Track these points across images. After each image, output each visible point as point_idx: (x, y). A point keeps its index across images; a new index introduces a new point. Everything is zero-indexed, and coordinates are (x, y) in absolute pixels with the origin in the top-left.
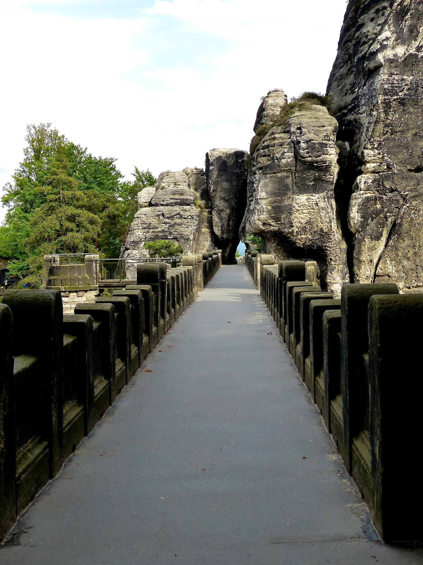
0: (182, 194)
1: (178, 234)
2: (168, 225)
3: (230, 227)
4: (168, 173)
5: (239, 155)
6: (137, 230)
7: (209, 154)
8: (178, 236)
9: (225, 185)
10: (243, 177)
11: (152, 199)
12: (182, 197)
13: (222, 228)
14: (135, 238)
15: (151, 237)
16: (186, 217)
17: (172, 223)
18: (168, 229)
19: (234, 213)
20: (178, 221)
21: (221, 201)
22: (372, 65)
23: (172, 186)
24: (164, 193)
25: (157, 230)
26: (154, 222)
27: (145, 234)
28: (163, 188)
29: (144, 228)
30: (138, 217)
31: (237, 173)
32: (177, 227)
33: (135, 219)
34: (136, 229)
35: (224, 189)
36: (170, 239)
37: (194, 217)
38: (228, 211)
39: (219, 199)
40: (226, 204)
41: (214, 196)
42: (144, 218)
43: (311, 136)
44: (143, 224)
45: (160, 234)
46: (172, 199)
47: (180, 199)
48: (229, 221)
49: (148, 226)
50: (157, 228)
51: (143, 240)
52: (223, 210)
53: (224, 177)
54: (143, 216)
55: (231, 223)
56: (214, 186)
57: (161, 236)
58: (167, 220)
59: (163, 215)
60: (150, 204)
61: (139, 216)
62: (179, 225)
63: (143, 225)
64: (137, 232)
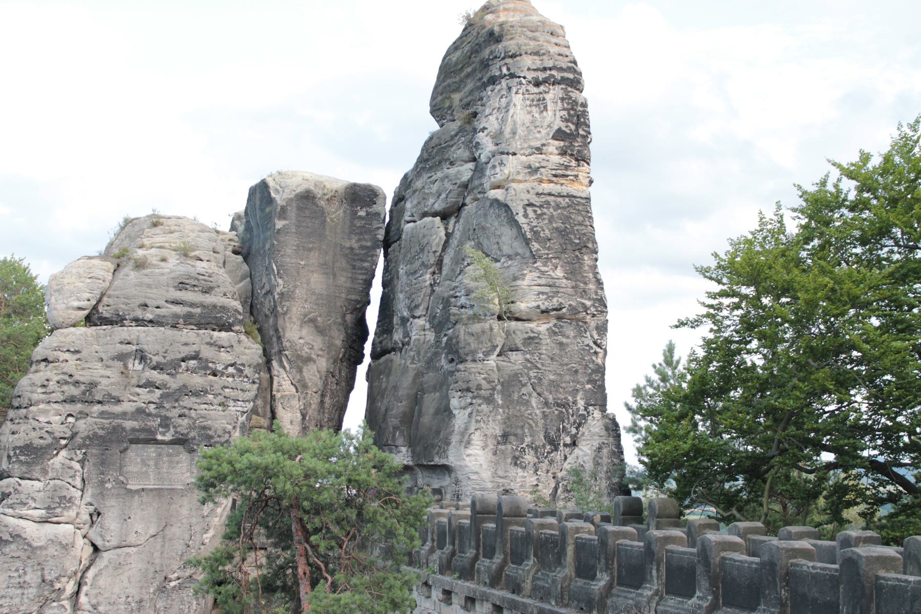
0: (207, 291)
1: (191, 428)
2: (158, 393)
3: (324, 413)
4: (156, 222)
5: (361, 196)
6: (42, 406)
7: (271, 183)
8: (192, 434)
9: (317, 281)
10: (366, 264)
11: (99, 301)
12: (209, 299)
13: (304, 416)
14: (33, 434)
15: (95, 434)
16: (220, 367)
17: (174, 384)
18: (160, 406)
19: (337, 372)
20: (197, 380)
21: (304, 332)
23: (173, 260)
24: (146, 280)
25: (117, 409)
26: (107, 378)
27: (70, 419)
28: (140, 265)
29: (72, 400)
30: (45, 360)
31: (352, 249)
32: (188, 401)
33: (34, 367)
34: (37, 403)
35: (313, 293)
36: (163, 443)
37: (247, 371)
38: (323, 364)
39: (298, 323)
40: (318, 342)
41: (285, 314)
42: (72, 364)
44: (67, 383)
45: (129, 424)
46: (175, 302)
47: (202, 306)
48: (323, 396)
49: (84, 393)
50: (118, 401)
51: (63, 442)
52: (309, 360)
53: (314, 258)
54: (67, 356)
55: (327, 400)
56: (285, 281)
57: (134, 430)
58: (155, 375)
59: (142, 356)
61: (51, 355)
62: (196, 394)
63: (65, 388)
64: (45, 412)
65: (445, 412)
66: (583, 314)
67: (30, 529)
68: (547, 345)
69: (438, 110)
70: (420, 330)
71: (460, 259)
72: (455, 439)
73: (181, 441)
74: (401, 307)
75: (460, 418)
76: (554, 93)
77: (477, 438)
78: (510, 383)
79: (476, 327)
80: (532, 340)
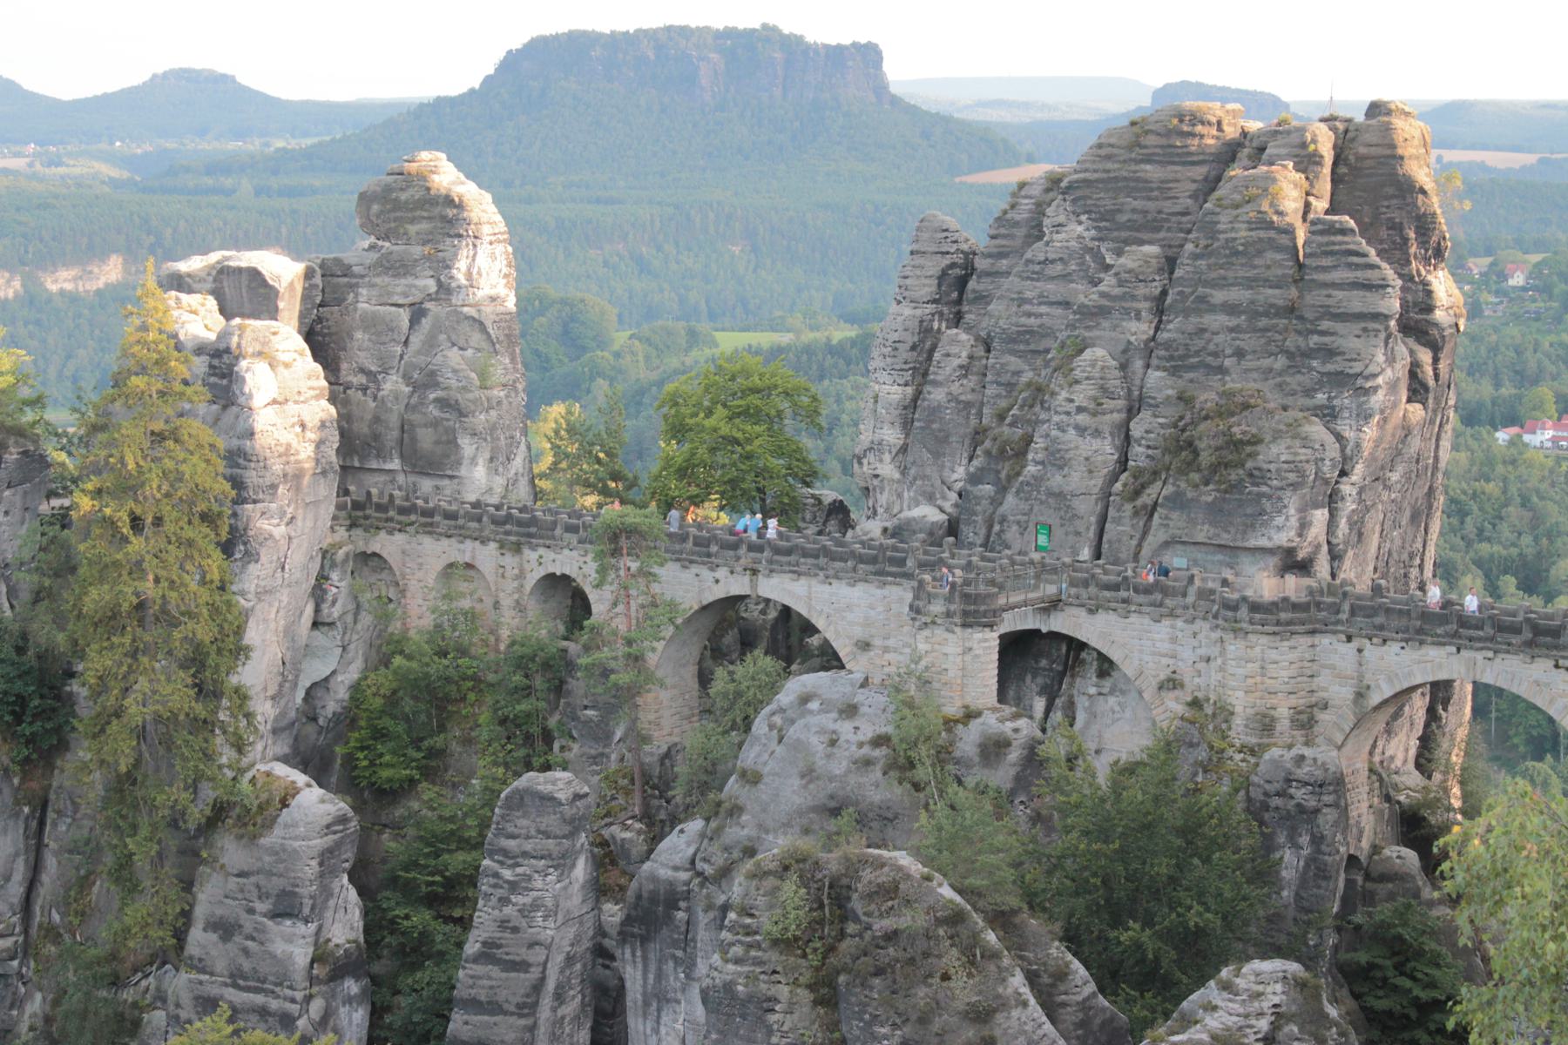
72: (466, 462)
77: (481, 461)
78: (493, 428)
79: (470, 396)
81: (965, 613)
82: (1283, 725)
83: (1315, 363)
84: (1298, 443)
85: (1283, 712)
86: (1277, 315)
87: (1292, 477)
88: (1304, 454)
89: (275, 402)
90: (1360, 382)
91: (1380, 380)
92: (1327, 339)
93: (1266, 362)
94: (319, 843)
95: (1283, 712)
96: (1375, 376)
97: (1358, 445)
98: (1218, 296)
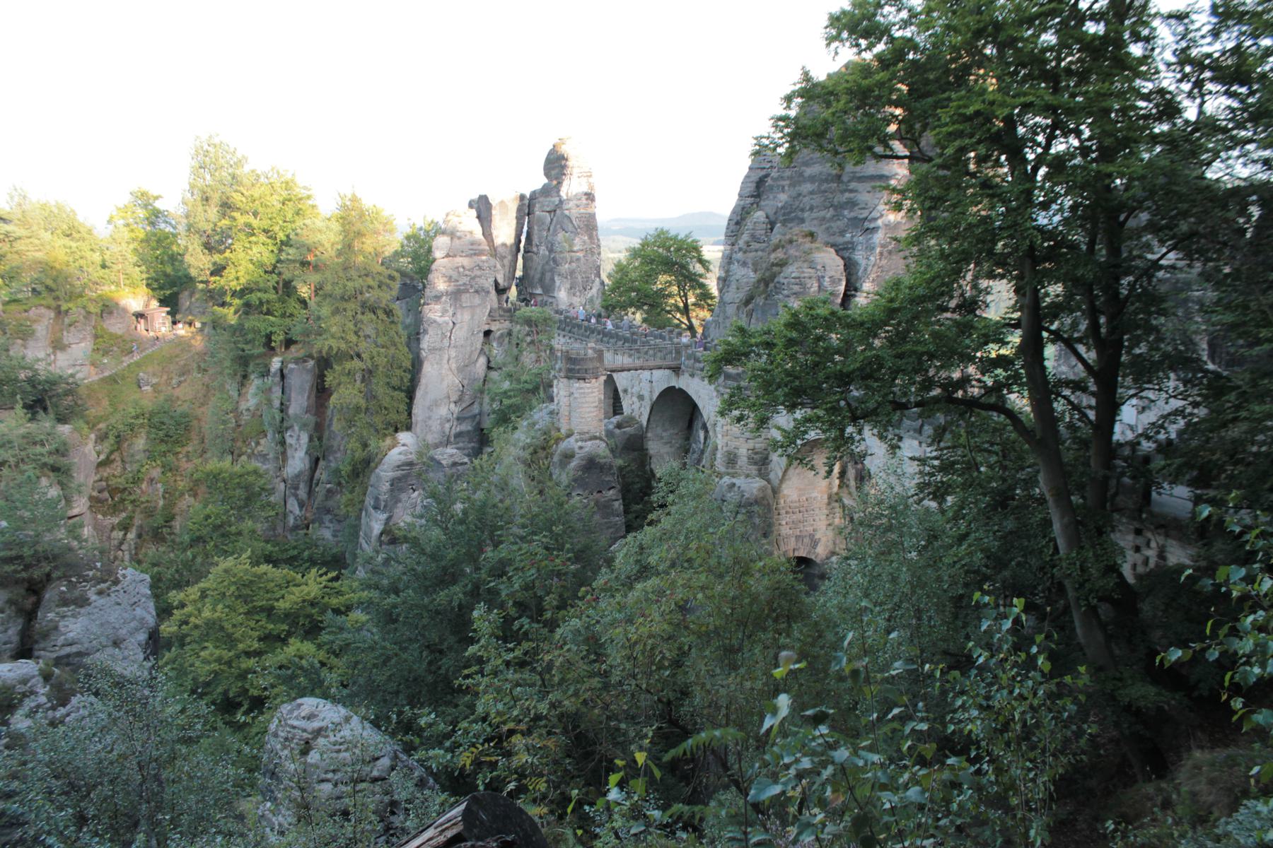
20: (479, 273)
22: (872, 226)
26: (455, 276)
28: (459, 238)
38: (509, 257)
43: (833, 273)
60: (448, 256)
65: (553, 280)
66: (594, 249)
67: (438, 319)
68: (583, 260)
69: (547, 174)
70: (543, 250)
71: (555, 230)
73: (477, 292)
74: (536, 240)
75: (558, 283)
76: (584, 180)
78: (572, 272)
80: (578, 259)
81: (570, 370)
82: (743, 461)
83: (846, 212)
84: (805, 265)
85: (743, 452)
86: (832, 181)
87: (796, 288)
88: (808, 272)
89: (448, 256)
90: (866, 224)
91: (880, 222)
92: (852, 195)
93: (822, 213)
94: (391, 474)
95: (743, 452)
96: (875, 219)
97: (865, 270)
98: (808, 171)
